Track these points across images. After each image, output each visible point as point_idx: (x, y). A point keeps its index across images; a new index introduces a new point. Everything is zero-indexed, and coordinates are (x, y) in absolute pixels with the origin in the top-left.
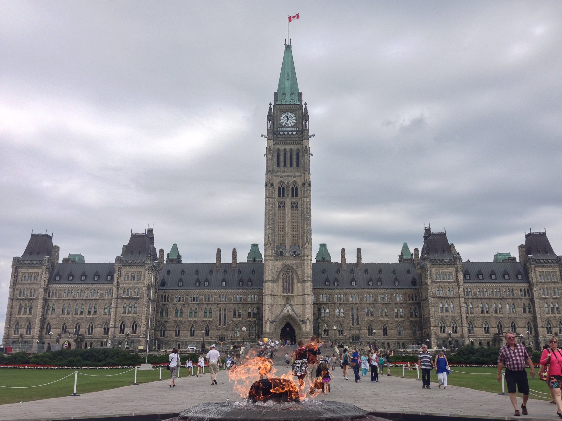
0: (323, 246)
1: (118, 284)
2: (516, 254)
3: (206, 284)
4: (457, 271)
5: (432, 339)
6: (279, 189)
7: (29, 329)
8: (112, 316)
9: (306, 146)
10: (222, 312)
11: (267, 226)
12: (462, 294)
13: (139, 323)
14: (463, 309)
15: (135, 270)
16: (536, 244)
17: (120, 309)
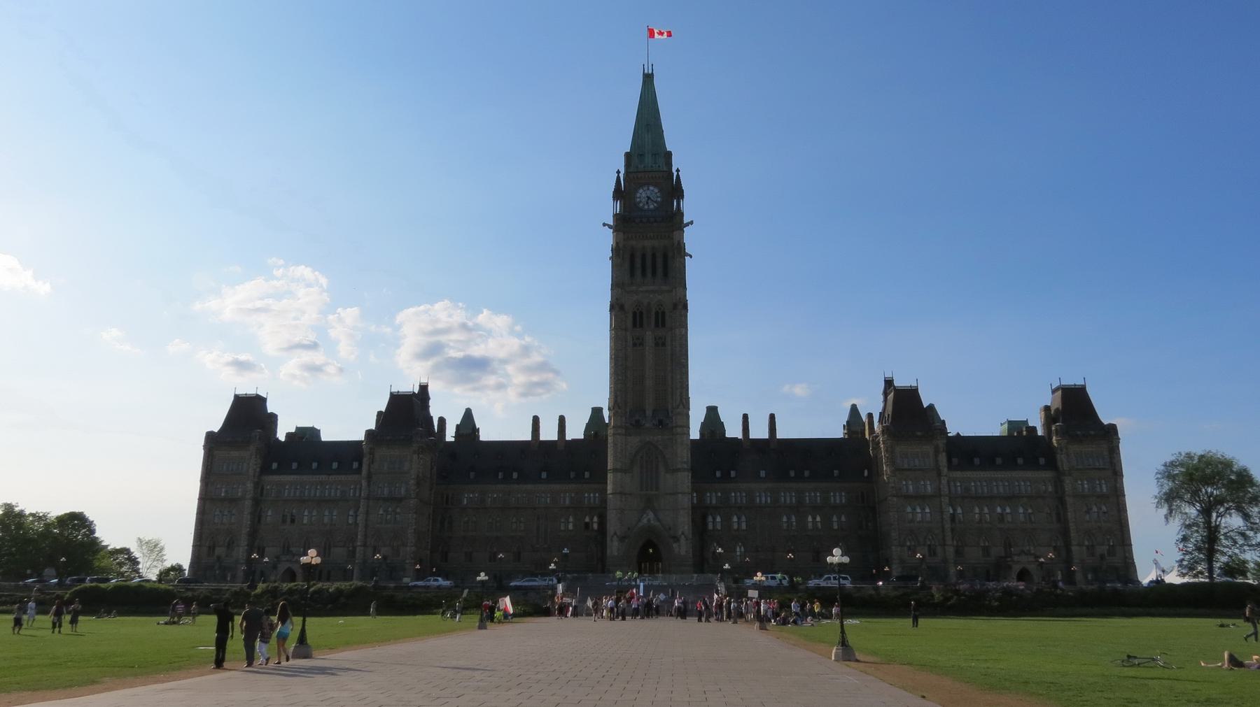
0: (712, 412)
1: (369, 477)
2: (1037, 422)
3: (515, 475)
4: (937, 452)
5: (894, 566)
6: (635, 314)
7: (230, 545)
8: (361, 528)
14: (947, 517)
16: (1074, 406)
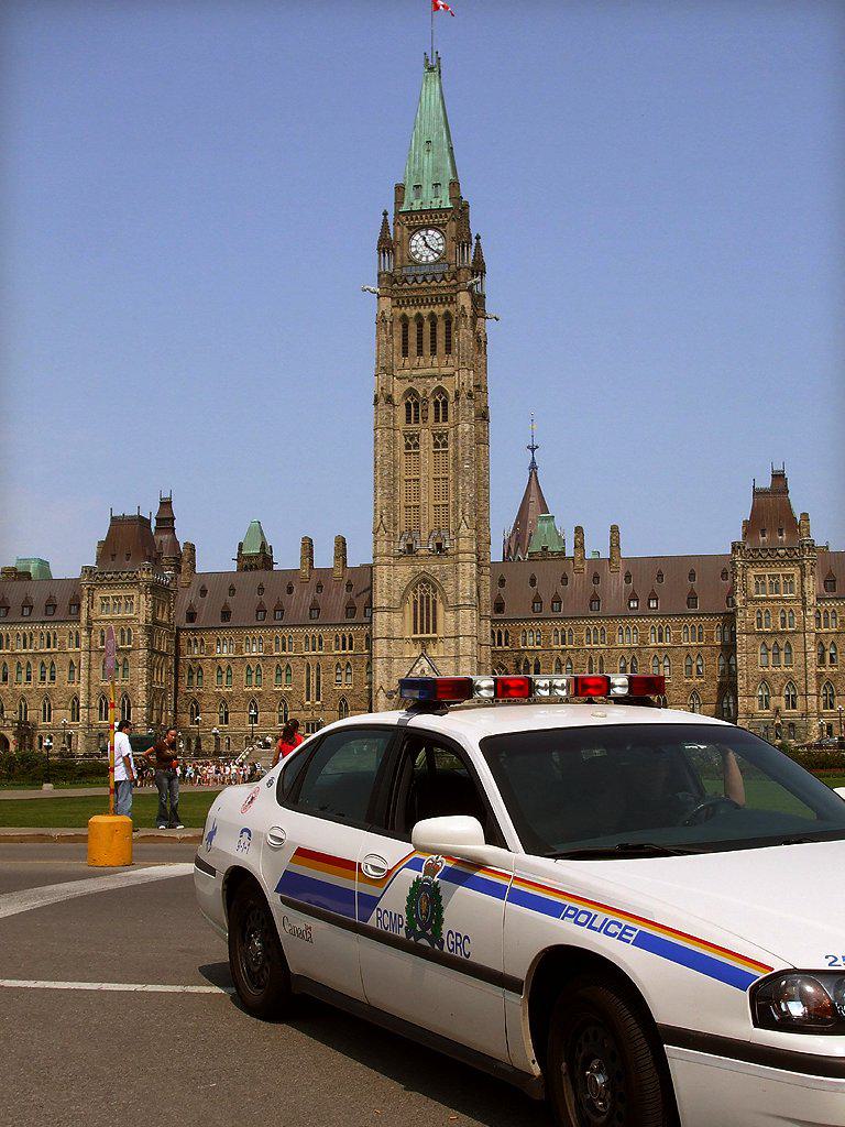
1: (90, 622)
4: (803, 575)
6: (408, 405)
9: (463, 307)
10: (313, 672)
11: (379, 490)
12: (811, 624)
17: (97, 672)
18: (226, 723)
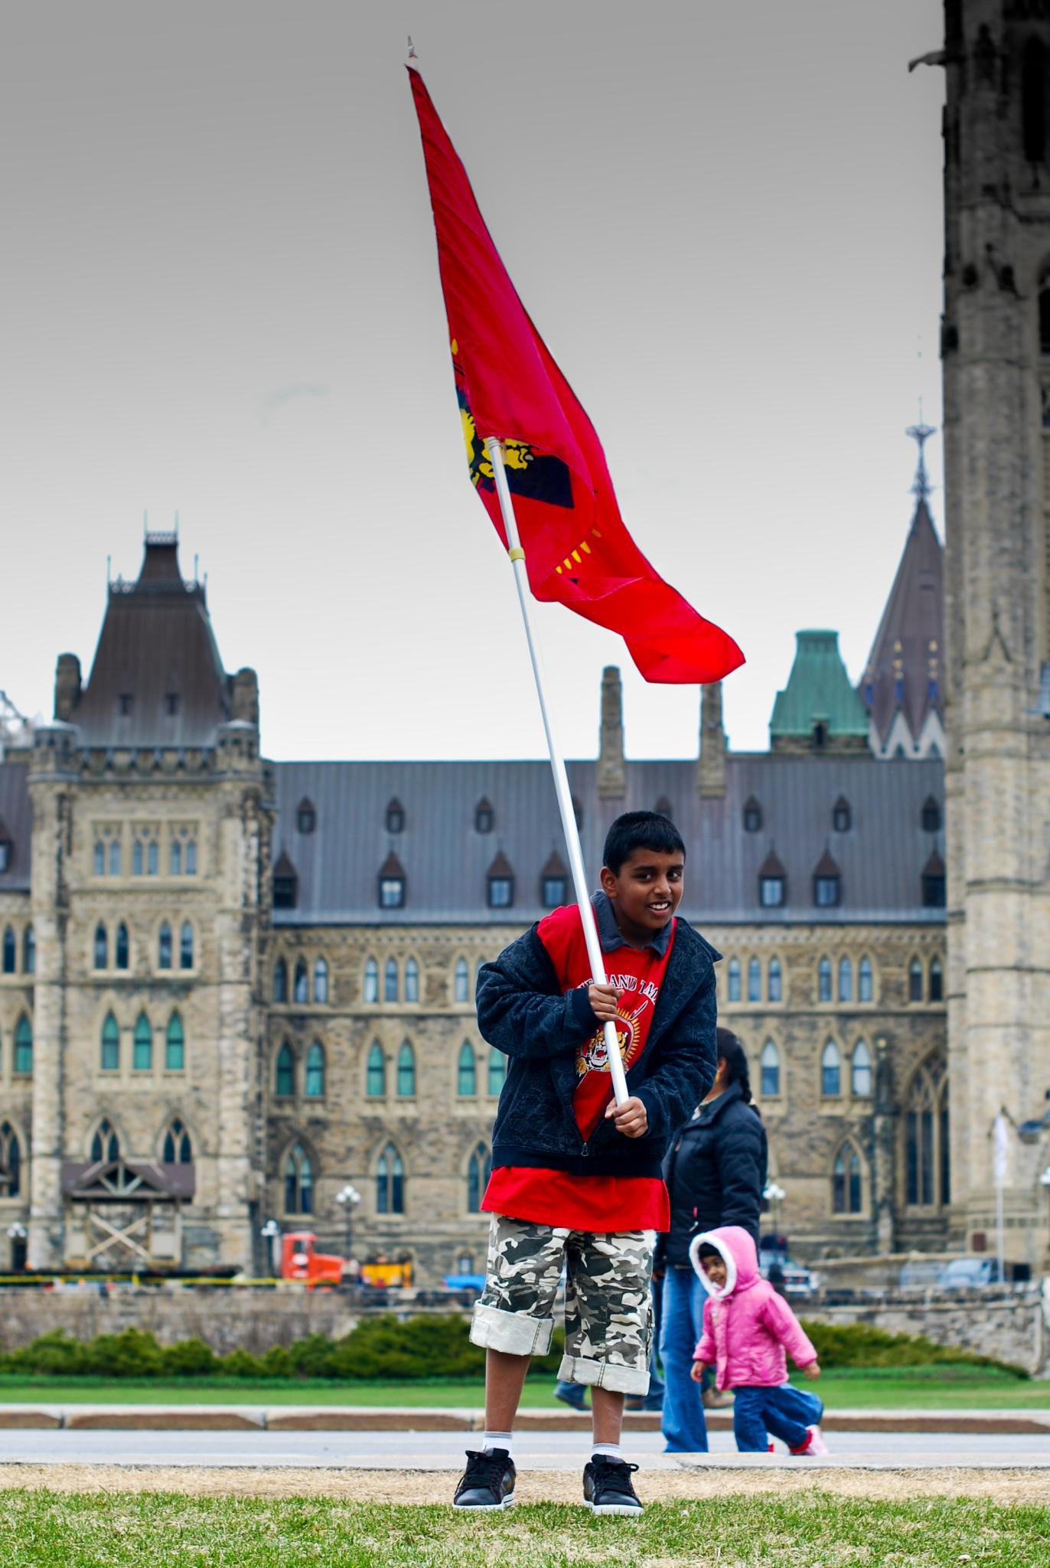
1: (62, 899)
8: (43, 1090)
13: (208, 1132)
15: (157, 810)
17: (86, 1048)
18: (399, 1206)
